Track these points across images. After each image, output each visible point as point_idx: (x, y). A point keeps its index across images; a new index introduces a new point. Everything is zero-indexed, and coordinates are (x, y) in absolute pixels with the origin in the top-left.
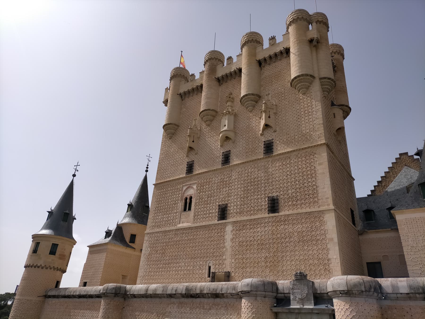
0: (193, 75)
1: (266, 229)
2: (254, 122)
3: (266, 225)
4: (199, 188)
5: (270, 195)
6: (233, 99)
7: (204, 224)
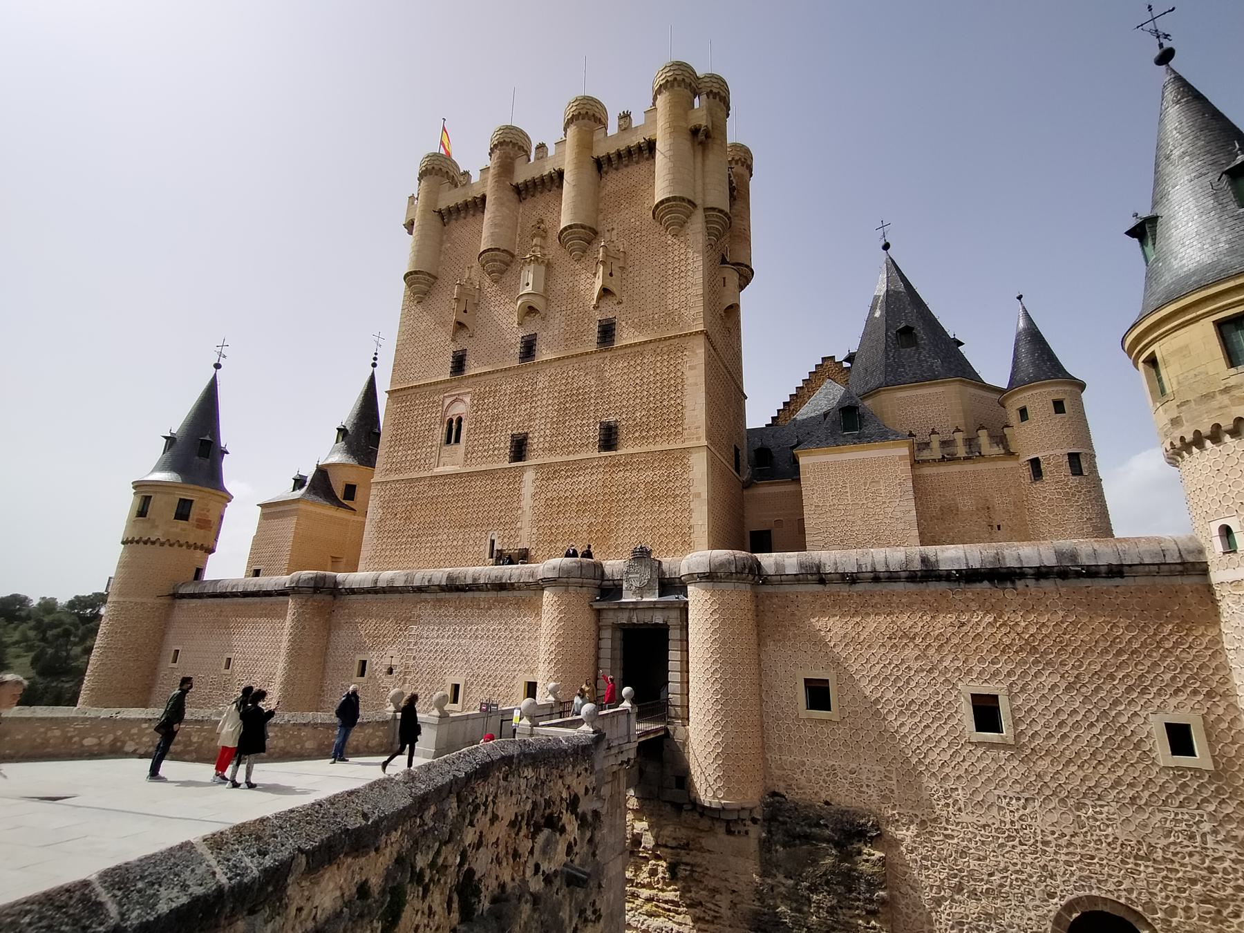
0: (466, 173)
1: (594, 477)
2: (582, 282)
3: (594, 470)
5: (604, 419)
6: (545, 231)
7: (484, 467)
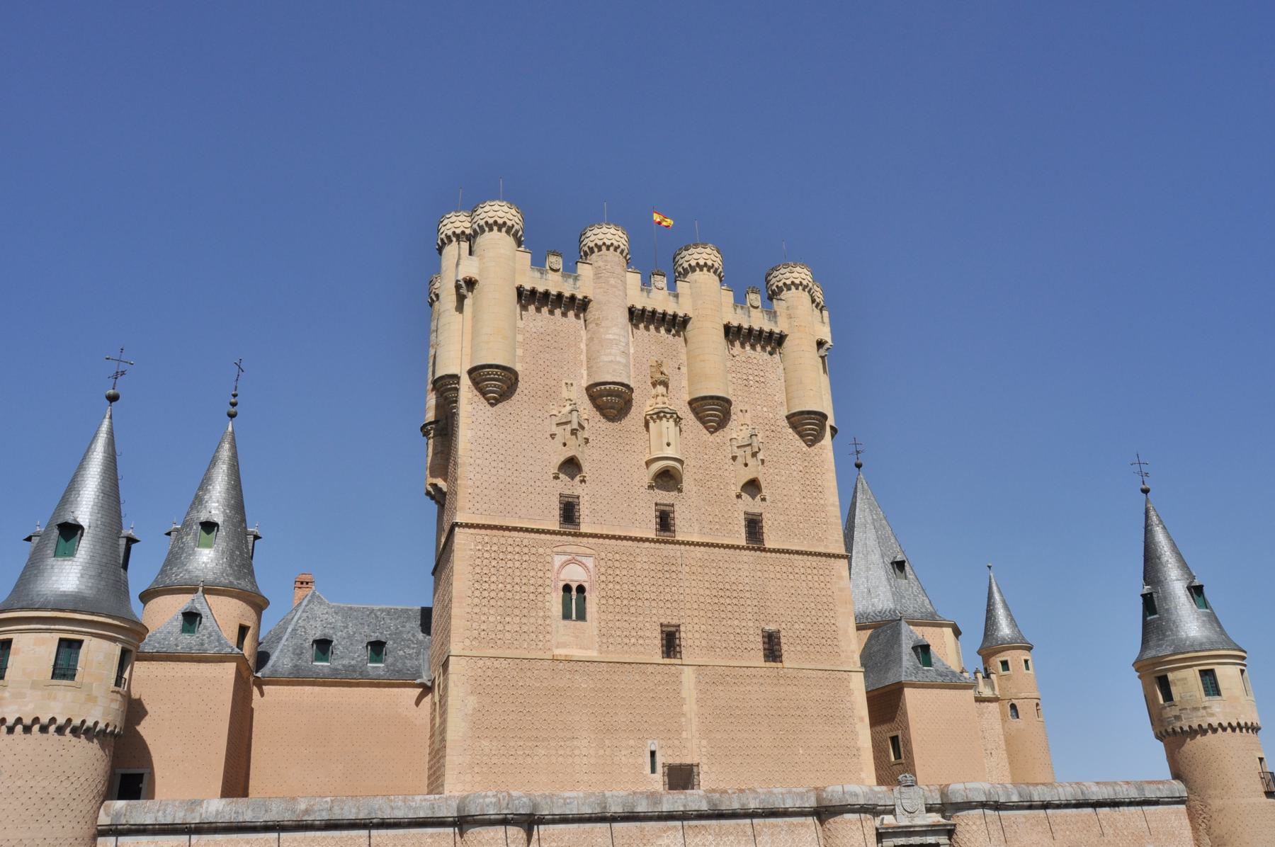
3: (761, 680)
4: (603, 570)
